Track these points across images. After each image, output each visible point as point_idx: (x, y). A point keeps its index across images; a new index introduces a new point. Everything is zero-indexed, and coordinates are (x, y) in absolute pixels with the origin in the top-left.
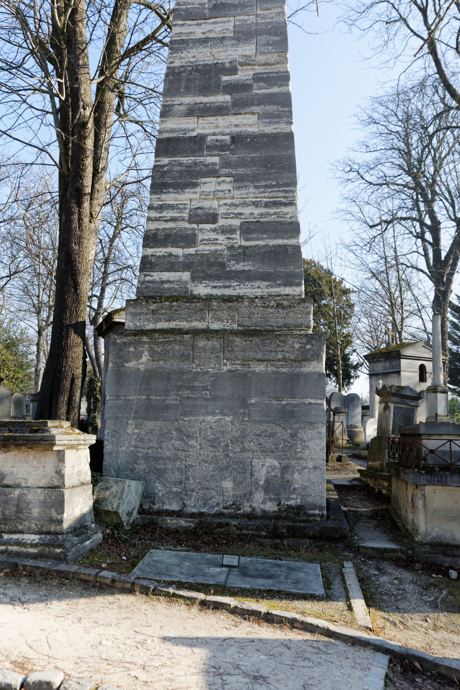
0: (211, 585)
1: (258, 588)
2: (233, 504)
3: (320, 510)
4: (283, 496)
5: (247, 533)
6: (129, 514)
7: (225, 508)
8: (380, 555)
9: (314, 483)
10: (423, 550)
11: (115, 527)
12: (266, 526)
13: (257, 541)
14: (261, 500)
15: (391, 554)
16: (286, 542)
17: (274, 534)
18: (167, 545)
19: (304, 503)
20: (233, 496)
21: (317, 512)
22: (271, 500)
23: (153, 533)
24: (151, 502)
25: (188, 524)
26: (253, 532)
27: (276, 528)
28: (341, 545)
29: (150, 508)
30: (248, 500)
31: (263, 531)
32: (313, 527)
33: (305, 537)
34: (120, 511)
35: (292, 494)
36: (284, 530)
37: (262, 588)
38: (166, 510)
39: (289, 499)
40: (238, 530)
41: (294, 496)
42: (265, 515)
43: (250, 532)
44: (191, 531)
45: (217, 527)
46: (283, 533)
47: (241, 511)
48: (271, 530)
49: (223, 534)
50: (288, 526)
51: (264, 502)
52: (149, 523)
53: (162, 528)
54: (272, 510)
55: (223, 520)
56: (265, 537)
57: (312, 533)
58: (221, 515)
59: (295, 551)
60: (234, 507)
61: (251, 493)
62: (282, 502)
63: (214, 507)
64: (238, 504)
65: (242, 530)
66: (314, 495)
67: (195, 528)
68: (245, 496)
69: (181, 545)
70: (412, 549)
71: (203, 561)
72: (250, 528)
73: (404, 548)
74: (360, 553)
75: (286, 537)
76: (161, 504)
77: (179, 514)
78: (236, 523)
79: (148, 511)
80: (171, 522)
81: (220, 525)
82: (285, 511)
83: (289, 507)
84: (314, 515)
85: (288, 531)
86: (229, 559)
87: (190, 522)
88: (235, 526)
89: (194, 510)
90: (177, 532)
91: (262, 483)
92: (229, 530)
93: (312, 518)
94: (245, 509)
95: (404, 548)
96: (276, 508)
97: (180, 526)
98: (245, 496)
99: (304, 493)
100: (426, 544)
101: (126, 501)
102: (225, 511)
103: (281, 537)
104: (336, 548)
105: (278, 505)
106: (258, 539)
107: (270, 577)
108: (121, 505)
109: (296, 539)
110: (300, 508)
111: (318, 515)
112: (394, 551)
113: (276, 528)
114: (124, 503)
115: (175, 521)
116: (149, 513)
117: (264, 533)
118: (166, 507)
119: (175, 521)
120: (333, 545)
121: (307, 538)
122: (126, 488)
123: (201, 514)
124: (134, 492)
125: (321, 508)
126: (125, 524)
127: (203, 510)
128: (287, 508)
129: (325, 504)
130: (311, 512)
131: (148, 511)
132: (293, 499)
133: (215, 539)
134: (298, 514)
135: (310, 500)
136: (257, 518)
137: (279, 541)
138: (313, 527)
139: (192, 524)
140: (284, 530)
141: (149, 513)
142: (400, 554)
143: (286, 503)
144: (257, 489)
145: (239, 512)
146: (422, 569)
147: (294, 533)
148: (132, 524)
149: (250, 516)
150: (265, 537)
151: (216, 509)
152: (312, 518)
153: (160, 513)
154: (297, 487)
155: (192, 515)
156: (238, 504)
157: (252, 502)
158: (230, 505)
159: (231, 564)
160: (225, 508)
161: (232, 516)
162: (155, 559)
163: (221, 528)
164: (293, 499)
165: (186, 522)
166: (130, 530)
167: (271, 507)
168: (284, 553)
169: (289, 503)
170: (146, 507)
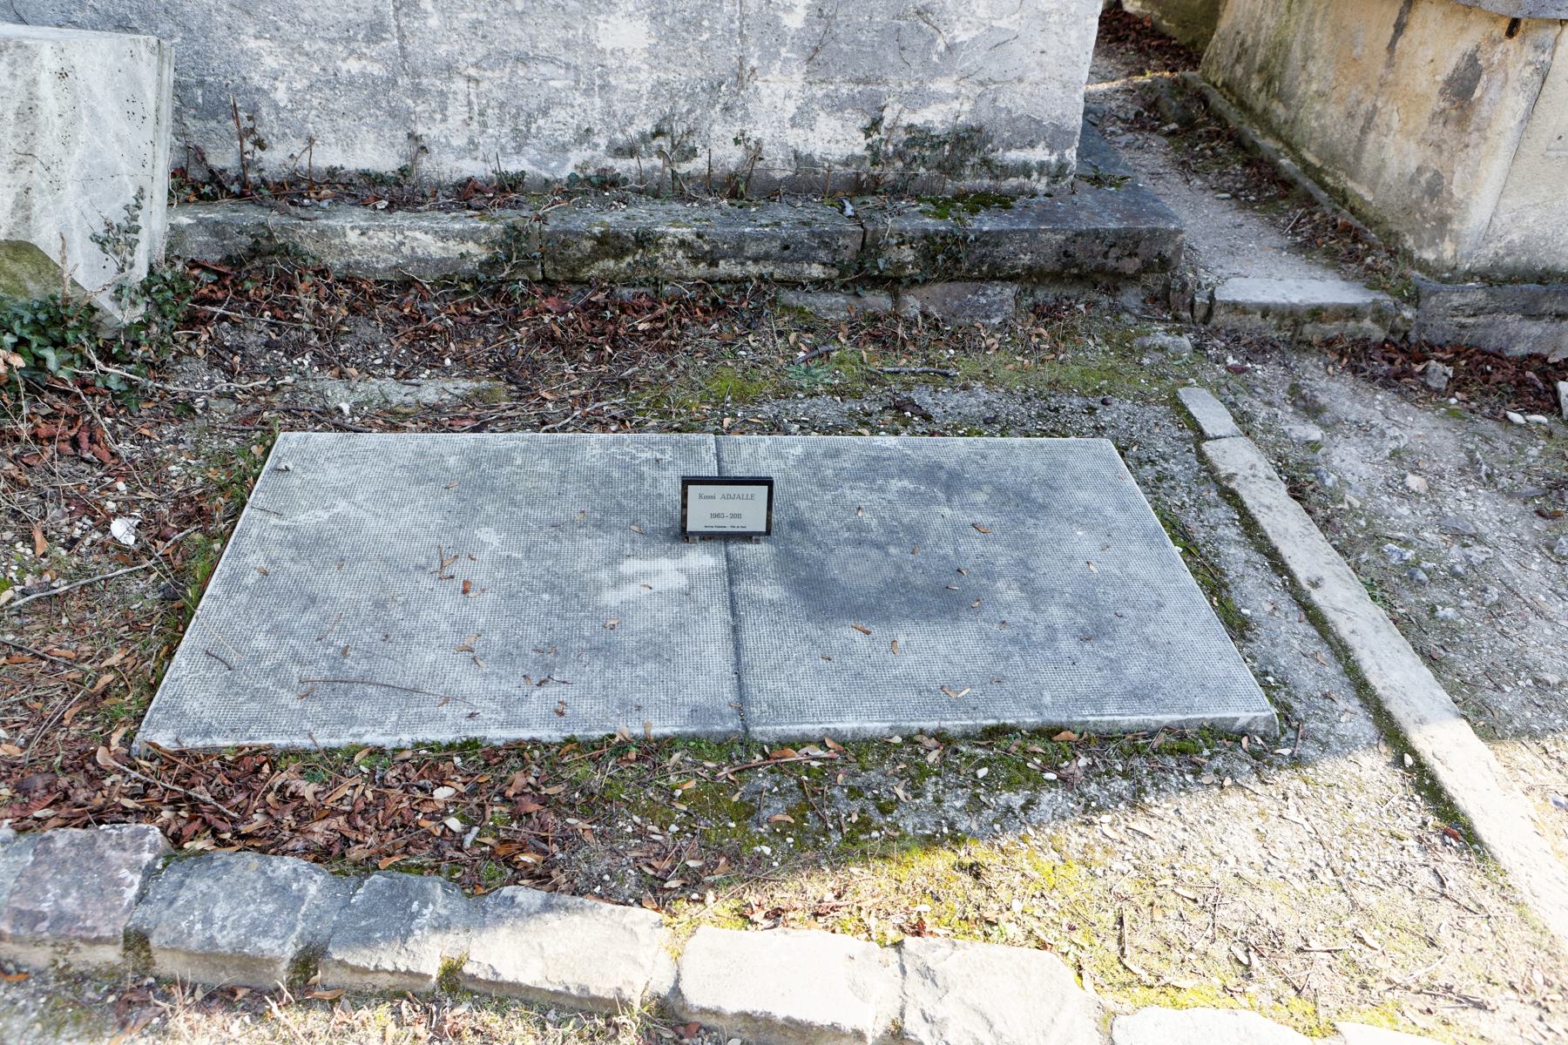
0: (666, 744)
1: (931, 725)
2: (659, 133)
3: (1051, 148)
4: (894, 85)
5: (737, 271)
6: (115, 239)
7: (619, 151)
8: (1294, 331)
9: (1045, 15)
10: (1456, 300)
11: (38, 327)
12: (826, 241)
13: (787, 308)
14: (791, 108)
15: (1332, 329)
16: (912, 304)
17: (863, 271)
18: (367, 370)
19: (986, 114)
20: (655, 94)
21: (1039, 154)
22: (836, 106)
23: (285, 312)
24: (243, 134)
25: (455, 248)
26: (767, 268)
27: (870, 247)
28: (1131, 298)
29: (245, 165)
30: (727, 109)
31: (811, 260)
32: (1034, 234)
33: (996, 274)
34: (45, 237)
35: (936, 73)
36: (907, 254)
37: (954, 724)
38: (332, 172)
39: (920, 98)
40: (695, 260)
41: (944, 85)
42: (808, 182)
43: (752, 269)
44: (473, 280)
45: (595, 256)
46: (902, 266)
47: (698, 165)
48: (847, 256)
49: (628, 282)
50: (926, 236)
51: (803, 118)
52: (255, 251)
53: (323, 272)
54: (838, 152)
55: (613, 218)
56: (820, 284)
57: (1026, 259)
58: (604, 185)
59: (962, 346)
60: (664, 143)
61: (741, 77)
62: (888, 116)
63: (564, 148)
64: (679, 128)
65: (713, 263)
66: (1036, 75)
67: (492, 264)
68: (714, 88)
69: (434, 361)
70: (1415, 299)
71: (571, 507)
72: (752, 249)
73: (1386, 300)
74: (1216, 331)
75: (914, 282)
76: (297, 146)
77: (397, 192)
78: (687, 233)
79: (241, 180)
80: (364, 239)
81: (609, 244)
82: (900, 155)
83: (919, 137)
84: (1025, 170)
85: (928, 256)
86: (719, 506)
87: (462, 237)
88: (683, 243)
89: (473, 168)
90: (407, 284)
91: (794, 21)
92: (653, 264)
93: (1013, 182)
94: (717, 153)
95: (1386, 300)
96: (858, 145)
97: (414, 258)
98: (714, 88)
99: (993, 69)
100: (1470, 275)
101: (70, 171)
102: (623, 166)
103: (893, 283)
104: (1117, 311)
105: (867, 132)
106: (789, 297)
107: (947, 598)
108: (38, 203)
109: (957, 288)
110: (967, 140)
111: (1043, 167)
112: (1353, 313)
113: (870, 247)
114: (56, 186)
115: (385, 238)
116: (246, 191)
117: (816, 271)
118: (327, 157)
119: (385, 238)
120: (1105, 301)
121: (1012, 279)
122: (47, 88)
123: (509, 187)
124: (110, 109)
125: (1057, 137)
126: (104, 302)
127: (512, 166)
128: (911, 143)
129: (1077, 122)
130: (1014, 156)
131: (241, 180)
132: (939, 98)
133: (593, 310)
134: (951, 168)
135: (1016, 100)
136: (772, 192)
137: (878, 301)
138: (1034, 234)
139: (471, 247)
140: (907, 254)
141: (246, 191)
142: (1367, 323)
143: (907, 119)
144: (770, 55)
145: (684, 168)
146: (1457, 384)
147: (946, 259)
148: (146, 289)
149: (736, 188)
150: (820, 284)
151: (576, 157)
152: (1013, 182)
153: (295, 189)
154: (962, 37)
155: (466, 194)
156: (679, 128)
157: (746, 117)
158: (644, 138)
159: (729, 525)
160: (619, 151)
161: (652, 191)
162: (308, 518)
163: (619, 254)
164: (939, 98)
165: (444, 236)
166: (145, 325)
167: (835, 140)
168: (917, 365)
169: (918, 119)
170: (224, 158)
